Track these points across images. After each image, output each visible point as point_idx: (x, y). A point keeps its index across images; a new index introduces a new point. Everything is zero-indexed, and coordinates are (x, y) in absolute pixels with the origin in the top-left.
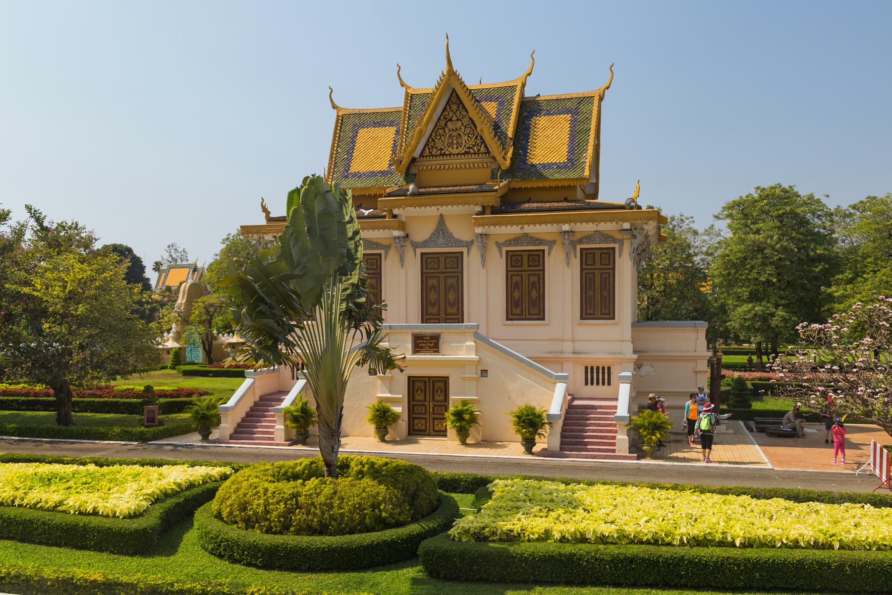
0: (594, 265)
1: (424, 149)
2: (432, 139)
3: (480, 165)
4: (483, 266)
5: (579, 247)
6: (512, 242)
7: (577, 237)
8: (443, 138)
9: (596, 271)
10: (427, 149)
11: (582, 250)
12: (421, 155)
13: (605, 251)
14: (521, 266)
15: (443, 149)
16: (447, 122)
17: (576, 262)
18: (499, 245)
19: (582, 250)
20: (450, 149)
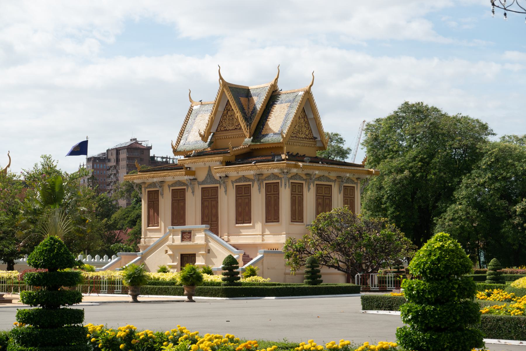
0: (271, 192)
1: (218, 128)
2: (221, 122)
3: (242, 136)
4: (226, 194)
5: (265, 182)
6: (238, 181)
7: (264, 177)
8: (226, 120)
9: (272, 196)
10: (219, 127)
11: (266, 184)
12: (217, 131)
13: (275, 184)
14: (242, 194)
15: (226, 127)
16: (228, 111)
17: (263, 190)
18: (233, 182)
19: (266, 184)
20: (229, 127)
